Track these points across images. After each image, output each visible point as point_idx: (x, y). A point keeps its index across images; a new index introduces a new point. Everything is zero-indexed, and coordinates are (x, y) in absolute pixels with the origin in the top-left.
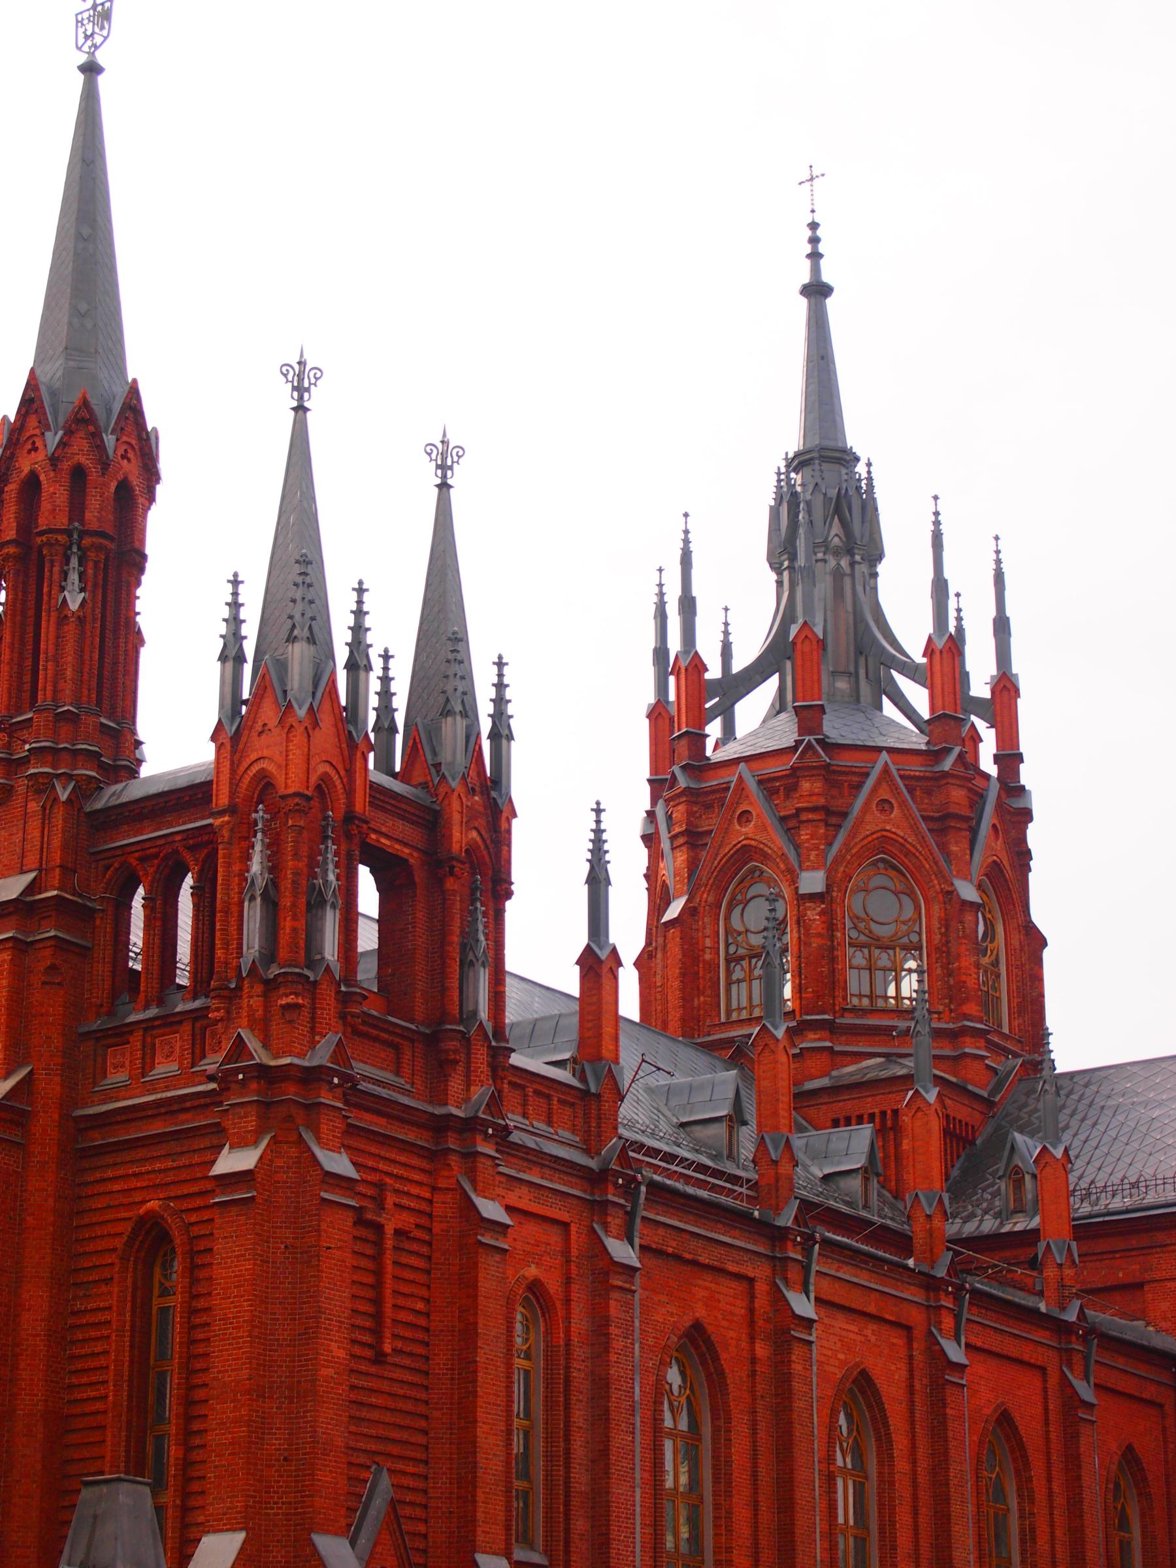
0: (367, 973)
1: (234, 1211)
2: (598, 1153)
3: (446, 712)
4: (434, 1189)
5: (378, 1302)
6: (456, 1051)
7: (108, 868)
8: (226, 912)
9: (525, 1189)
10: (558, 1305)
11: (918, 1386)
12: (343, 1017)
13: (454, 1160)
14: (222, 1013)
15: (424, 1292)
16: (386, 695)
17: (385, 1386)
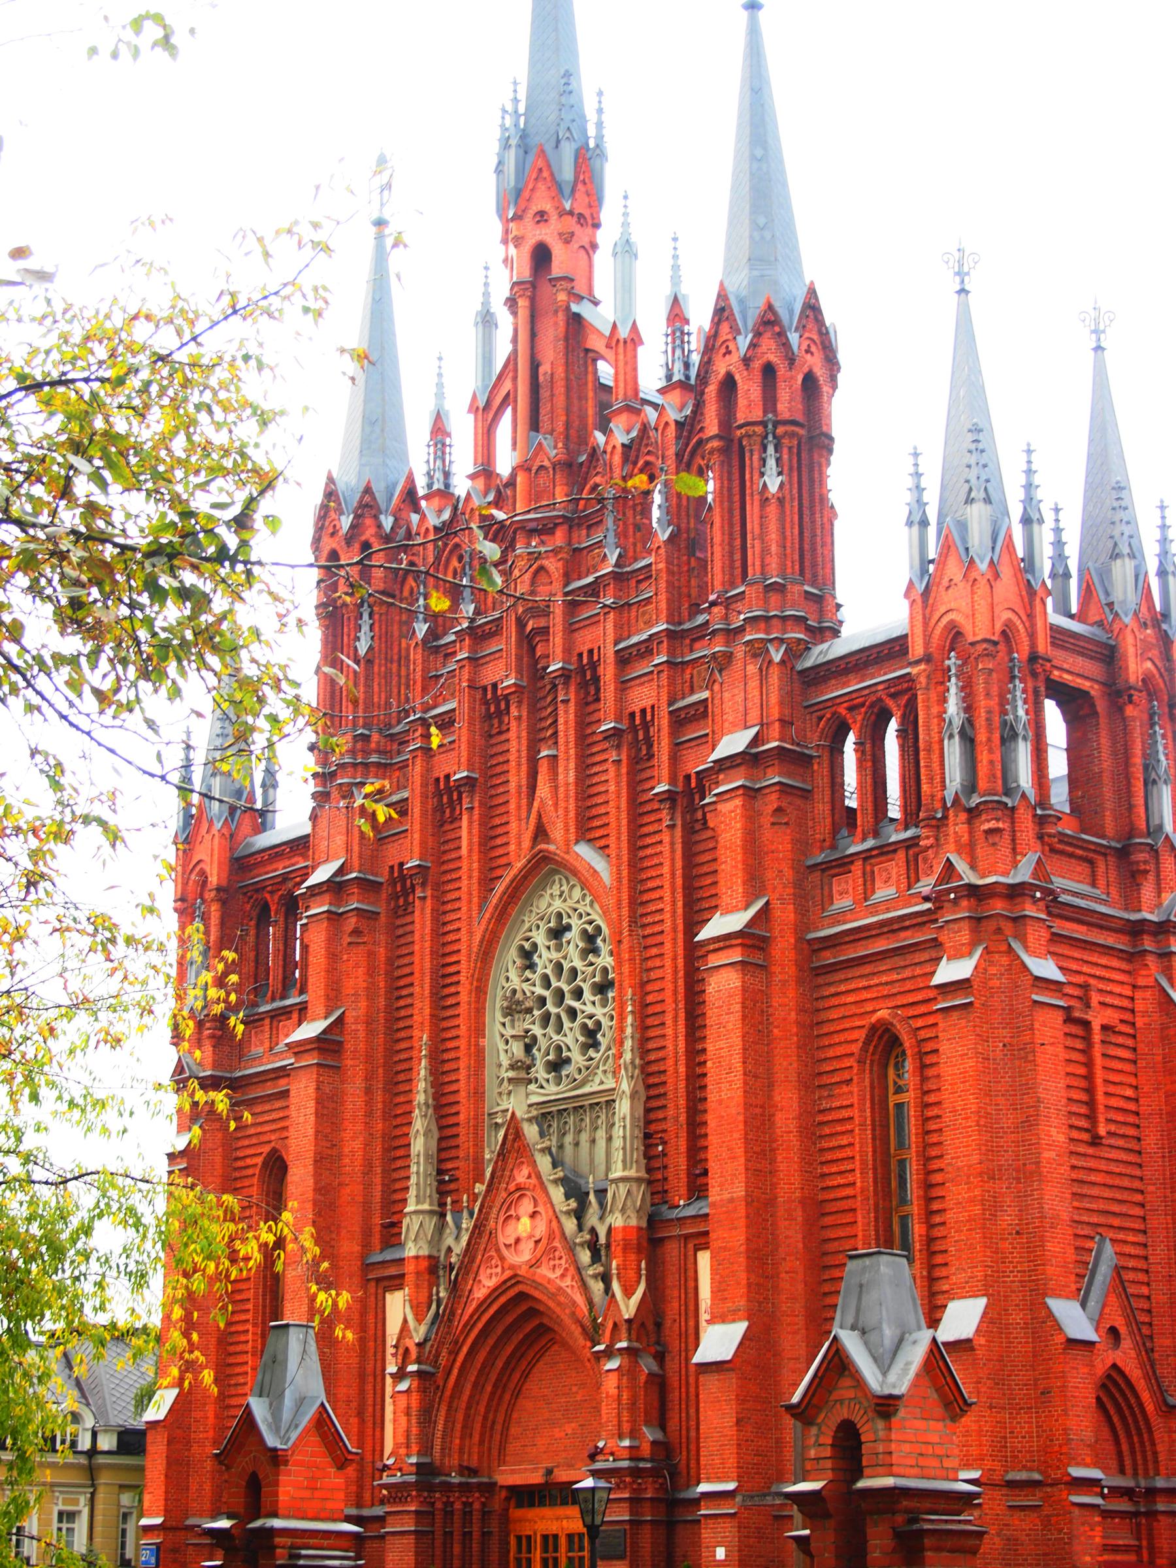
0: (1060, 797)
1: (955, 1015)
3: (1115, 556)
4: (1134, 987)
5: (1090, 1090)
6: (1145, 862)
7: (820, 718)
8: (929, 750)
12: (1040, 837)
13: (1150, 960)
14: (931, 841)
15: (1131, 1080)
16: (1059, 544)
17: (1103, 1166)
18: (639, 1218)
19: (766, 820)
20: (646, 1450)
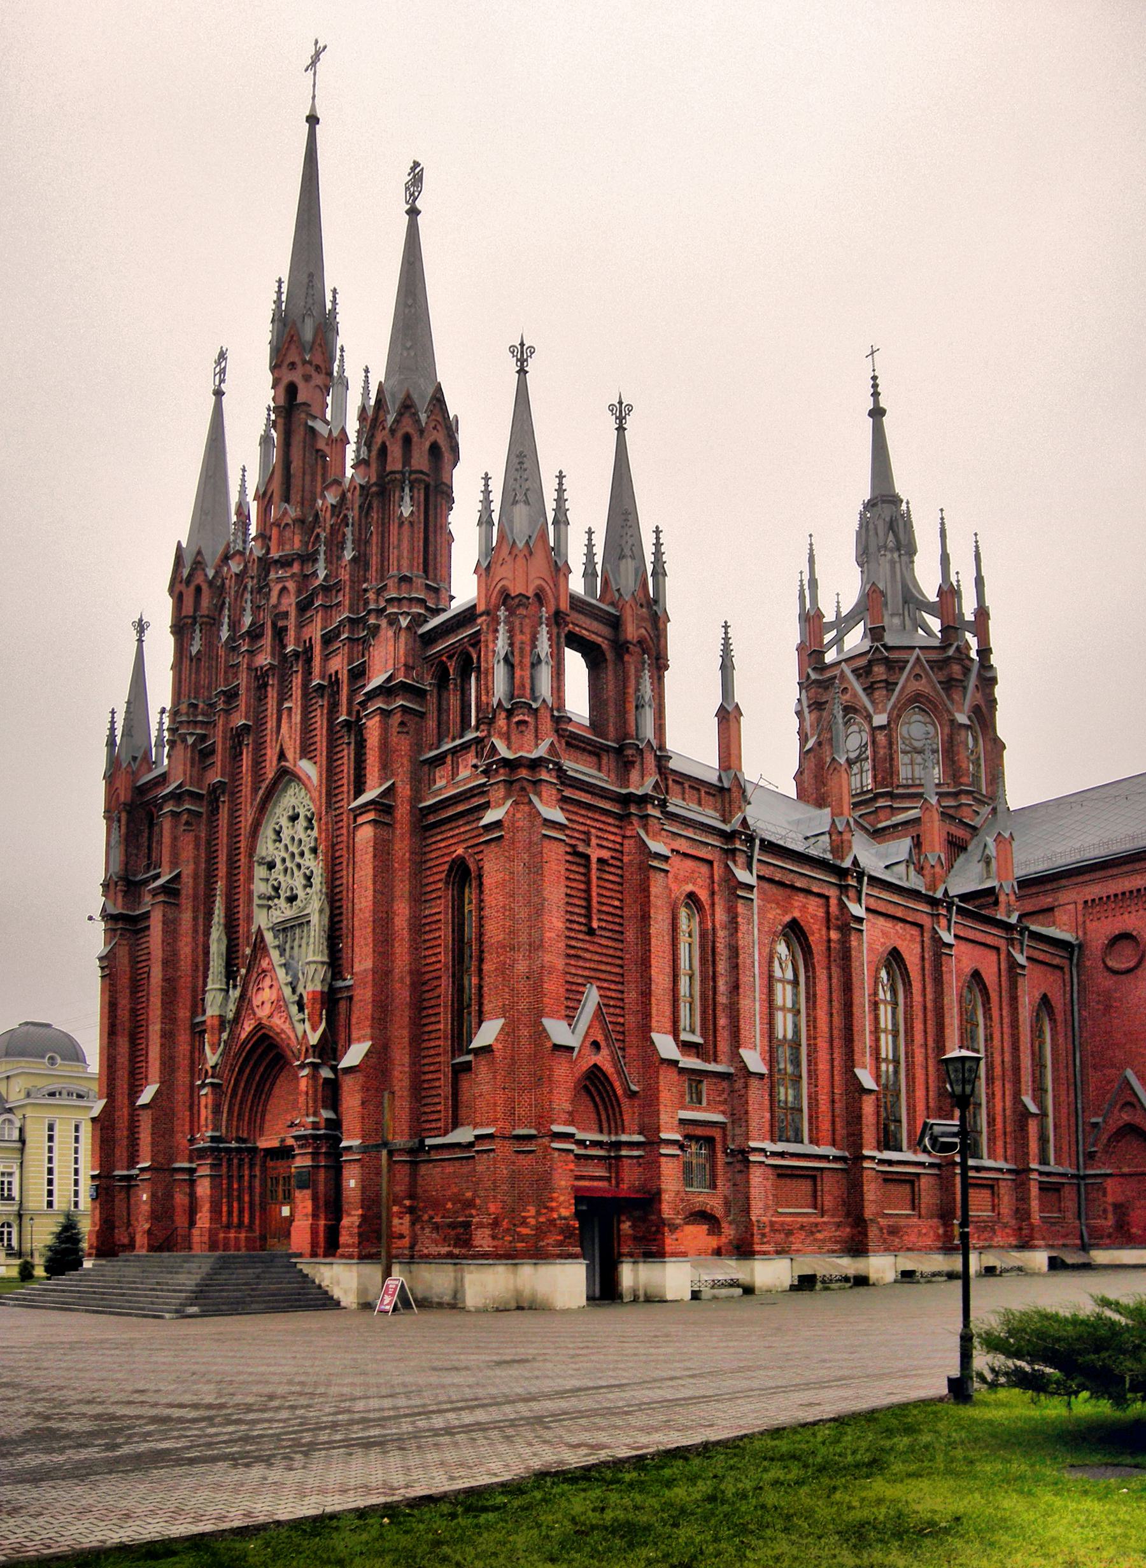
1: (493, 845)
2: (730, 822)
4: (624, 837)
5: (588, 900)
6: (633, 756)
9: (683, 840)
10: (707, 907)
11: (926, 956)
12: (557, 731)
13: (635, 820)
18: (323, 986)
19: (395, 729)
20: (323, 1125)
